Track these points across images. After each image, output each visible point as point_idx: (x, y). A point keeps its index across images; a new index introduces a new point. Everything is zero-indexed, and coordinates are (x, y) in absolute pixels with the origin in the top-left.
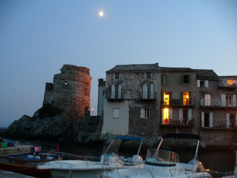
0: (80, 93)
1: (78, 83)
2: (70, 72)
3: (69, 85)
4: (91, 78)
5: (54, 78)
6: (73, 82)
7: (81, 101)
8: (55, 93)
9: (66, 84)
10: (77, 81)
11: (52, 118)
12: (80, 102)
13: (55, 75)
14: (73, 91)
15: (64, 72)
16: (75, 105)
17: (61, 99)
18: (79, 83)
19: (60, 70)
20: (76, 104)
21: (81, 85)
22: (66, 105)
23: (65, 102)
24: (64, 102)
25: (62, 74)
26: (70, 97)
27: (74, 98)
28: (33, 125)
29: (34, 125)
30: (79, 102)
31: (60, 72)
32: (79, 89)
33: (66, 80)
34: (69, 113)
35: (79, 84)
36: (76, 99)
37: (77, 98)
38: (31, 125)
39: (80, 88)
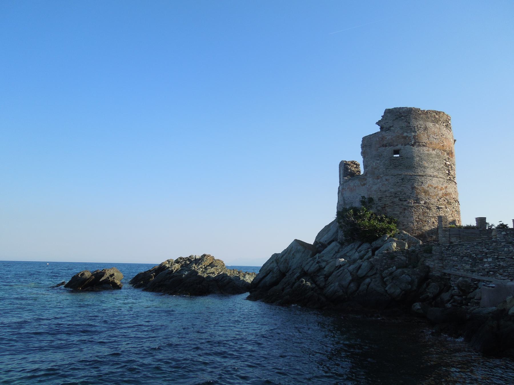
1: (428, 150)
2: (404, 125)
3: (407, 158)
5: (363, 146)
7: (440, 195)
11: (371, 243)
13: (364, 139)
15: (388, 127)
18: (431, 150)
21: (438, 156)
22: (405, 209)
23: (400, 200)
24: (396, 200)
25: (383, 133)
28: (323, 264)
29: (327, 264)
31: (377, 129)
33: (397, 145)
35: (431, 154)
38: (318, 262)
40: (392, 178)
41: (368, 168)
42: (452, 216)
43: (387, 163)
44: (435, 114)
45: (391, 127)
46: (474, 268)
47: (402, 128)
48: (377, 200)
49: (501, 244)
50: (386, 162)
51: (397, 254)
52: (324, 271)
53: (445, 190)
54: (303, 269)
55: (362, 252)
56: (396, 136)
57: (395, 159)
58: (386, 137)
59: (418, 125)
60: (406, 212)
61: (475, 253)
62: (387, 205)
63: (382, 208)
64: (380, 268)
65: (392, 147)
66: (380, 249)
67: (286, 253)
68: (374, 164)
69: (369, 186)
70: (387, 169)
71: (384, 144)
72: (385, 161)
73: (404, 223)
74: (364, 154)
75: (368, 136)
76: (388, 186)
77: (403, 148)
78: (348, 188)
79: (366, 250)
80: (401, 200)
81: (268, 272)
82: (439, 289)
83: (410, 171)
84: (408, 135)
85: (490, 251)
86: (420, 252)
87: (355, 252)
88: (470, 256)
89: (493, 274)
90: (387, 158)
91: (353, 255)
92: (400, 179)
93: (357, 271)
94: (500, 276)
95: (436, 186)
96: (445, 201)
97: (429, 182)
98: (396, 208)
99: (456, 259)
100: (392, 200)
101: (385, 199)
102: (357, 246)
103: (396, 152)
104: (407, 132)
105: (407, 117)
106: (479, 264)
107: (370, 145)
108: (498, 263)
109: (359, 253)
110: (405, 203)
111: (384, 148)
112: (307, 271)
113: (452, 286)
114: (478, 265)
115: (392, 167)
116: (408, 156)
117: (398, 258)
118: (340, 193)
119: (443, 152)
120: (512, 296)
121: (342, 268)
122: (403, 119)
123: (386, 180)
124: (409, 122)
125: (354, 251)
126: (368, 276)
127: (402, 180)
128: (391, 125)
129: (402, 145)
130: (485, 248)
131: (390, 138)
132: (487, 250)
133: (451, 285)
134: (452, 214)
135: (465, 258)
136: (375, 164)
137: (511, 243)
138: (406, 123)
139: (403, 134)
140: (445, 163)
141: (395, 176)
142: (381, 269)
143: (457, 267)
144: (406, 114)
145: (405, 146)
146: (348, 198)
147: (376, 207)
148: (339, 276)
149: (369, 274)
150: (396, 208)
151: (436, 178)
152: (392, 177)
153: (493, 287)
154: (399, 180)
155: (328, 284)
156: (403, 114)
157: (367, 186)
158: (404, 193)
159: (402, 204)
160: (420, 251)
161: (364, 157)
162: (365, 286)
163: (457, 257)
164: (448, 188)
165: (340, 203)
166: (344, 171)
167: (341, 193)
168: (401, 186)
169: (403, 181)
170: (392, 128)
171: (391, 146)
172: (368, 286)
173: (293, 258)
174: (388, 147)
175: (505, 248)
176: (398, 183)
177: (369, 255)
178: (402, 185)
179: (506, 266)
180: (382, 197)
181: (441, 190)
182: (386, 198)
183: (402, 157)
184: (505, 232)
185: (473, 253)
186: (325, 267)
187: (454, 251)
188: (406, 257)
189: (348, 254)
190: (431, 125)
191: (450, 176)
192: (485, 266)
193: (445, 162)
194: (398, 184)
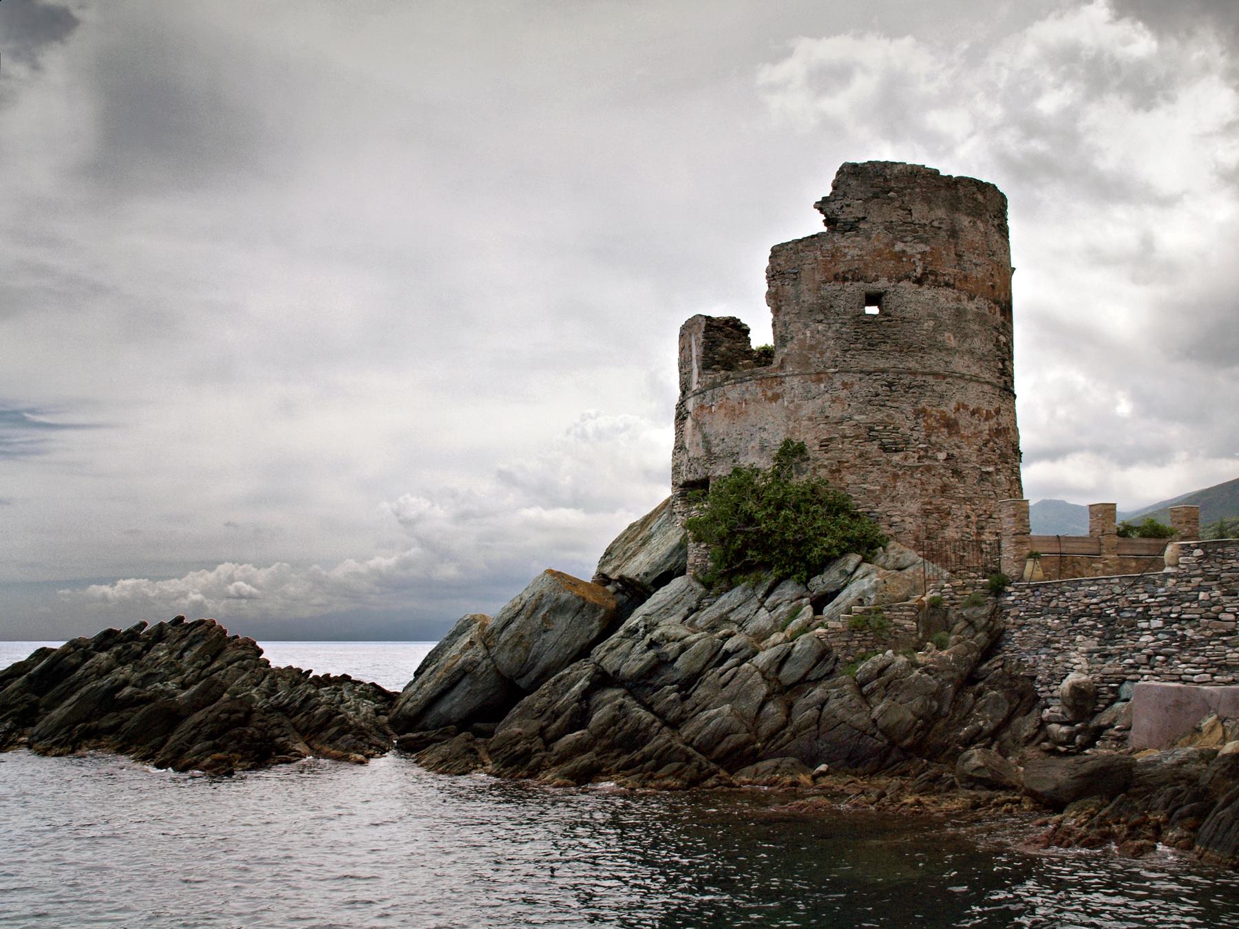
0: (975, 379)
1: (959, 300)
4: (1014, 269)
5: (774, 275)
6: (927, 293)
8: (794, 384)
9: (873, 310)
10: (953, 286)
12: (985, 445)
16: (956, 473)
17: (846, 428)
18: (964, 297)
20: (961, 466)
21: (980, 317)
22: (895, 476)
23: (884, 448)
24: (873, 447)
25: (837, 237)
27: (943, 415)
29: (683, 649)
30: (980, 450)
32: (966, 345)
33: (876, 279)
35: (965, 310)
36: (956, 423)
37: (964, 419)
38: (652, 644)
40: (860, 379)
41: (789, 345)
43: (847, 333)
44: (975, 189)
46: (1109, 647)
48: (817, 448)
49: (1189, 582)
50: (844, 329)
51: (894, 613)
52: (676, 670)
53: (995, 419)
55: (782, 609)
56: (874, 251)
57: (870, 323)
58: (847, 250)
59: (933, 221)
60: (898, 484)
61: (1114, 606)
62: (846, 464)
63: (832, 472)
64: (846, 655)
65: (861, 283)
66: (837, 600)
67: (518, 614)
68: (808, 334)
69: (793, 401)
71: (838, 274)
72: (841, 328)
73: (894, 519)
74: (775, 299)
75: (789, 243)
76: (849, 405)
77: (893, 289)
78: (720, 407)
79: (792, 602)
83: (910, 359)
84: (908, 249)
85: (1159, 599)
86: (953, 605)
87: (759, 608)
88: (1101, 616)
89: (1163, 662)
90: (849, 317)
91: (751, 617)
92: (882, 386)
93: (779, 670)
94: (1184, 666)
96: (994, 451)
98: (871, 472)
99: (1057, 621)
100: (859, 447)
101: (840, 446)
102: (762, 592)
103: (873, 299)
104: (905, 239)
105: (905, 195)
106: (1125, 635)
107: (795, 274)
108: (1179, 633)
109: (770, 611)
110: (896, 458)
113: (1040, 698)
114: (1122, 638)
115: (860, 346)
116: (907, 315)
117: (896, 625)
119: (992, 304)
120: (1215, 716)
121: (730, 662)
123: (845, 385)
124: (910, 210)
125: (754, 605)
126: (809, 681)
127: (888, 389)
128: (861, 216)
129: (890, 280)
130: (1145, 592)
131: (858, 256)
133: (1039, 694)
134: (1009, 490)
135: (1084, 619)
136: (812, 332)
137: (1216, 580)
138: (901, 212)
140: (997, 338)
141: (870, 373)
142: (849, 658)
143: (1057, 645)
144: (902, 186)
145: (899, 282)
146: (722, 437)
147: (814, 469)
148: (725, 685)
149: (813, 676)
150: (871, 472)
151: (975, 385)
152: (860, 375)
154: (879, 387)
155: (693, 709)
156: (893, 184)
157: (786, 403)
158: (894, 428)
159: (889, 462)
160: (953, 602)
161: (776, 310)
163: (1058, 619)
164: (1002, 412)
165: (691, 454)
166: (705, 348)
167: (696, 420)
168: (884, 405)
169: (891, 391)
170: (861, 226)
171: (858, 281)
173: (545, 631)
174: (849, 283)
175: (1199, 591)
177: (805, 618)
178: (889, 404)
179: (1202, 640)
180: (830, 440)
181: (986, 419)
182: (843, 443)
183: (889, 315)
184: (1203, 549)
185: (1109, 606)
186: (675, 659)
187: (1049, 602)
188: (917, 622)
189: (733, 617)
190: (966, 223)
191: (1006, 379)
192: (1141, 640)
193: (996, 334)
194: (877, 398)
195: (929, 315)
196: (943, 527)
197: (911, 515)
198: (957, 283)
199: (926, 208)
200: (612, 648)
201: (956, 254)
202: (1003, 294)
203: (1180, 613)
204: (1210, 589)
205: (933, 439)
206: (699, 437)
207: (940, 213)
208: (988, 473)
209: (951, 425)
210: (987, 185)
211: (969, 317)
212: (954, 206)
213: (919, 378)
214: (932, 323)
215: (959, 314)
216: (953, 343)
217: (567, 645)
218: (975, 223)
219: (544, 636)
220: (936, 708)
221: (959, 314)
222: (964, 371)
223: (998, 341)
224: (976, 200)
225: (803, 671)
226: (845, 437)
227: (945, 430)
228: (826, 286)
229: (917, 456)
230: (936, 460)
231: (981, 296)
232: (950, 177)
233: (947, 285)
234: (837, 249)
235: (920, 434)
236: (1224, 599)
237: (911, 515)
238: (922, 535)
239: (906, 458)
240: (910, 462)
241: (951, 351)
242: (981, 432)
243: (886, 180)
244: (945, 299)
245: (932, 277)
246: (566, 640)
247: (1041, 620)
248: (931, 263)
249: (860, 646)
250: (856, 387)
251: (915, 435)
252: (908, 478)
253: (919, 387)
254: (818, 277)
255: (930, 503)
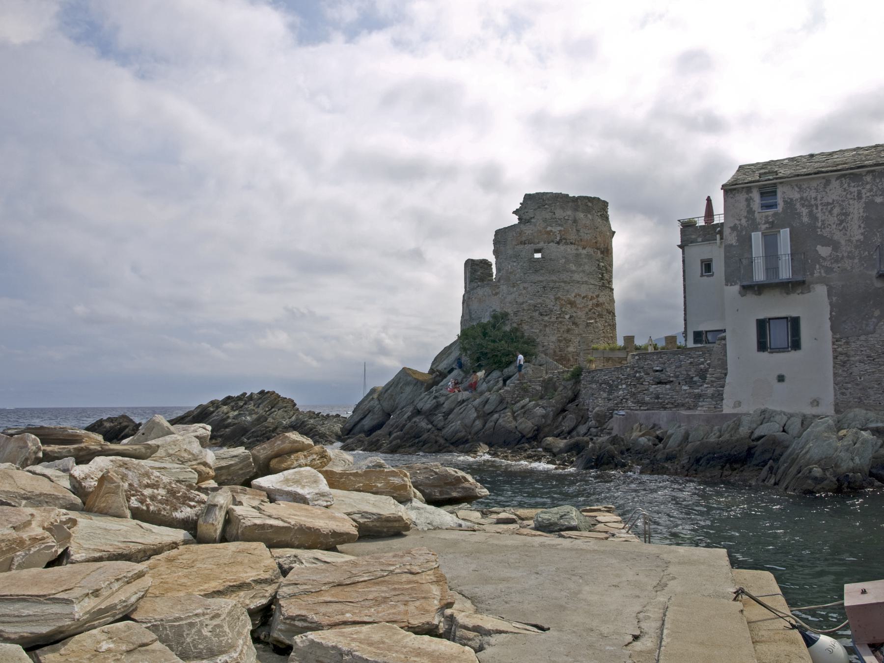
0: (586, 283)
1: (577, 249)
2: (548, 216)
3: (551, 259)
4: (614, 232)
5: (496, 242)
6: (562, 247)
7: (590, 307)
9: (538, 256)
10: (575, 244)
12: (590, 311)
13: (498, 232)
14: (565, 276)
15: (528, 218)
16: (574, 323)
17: (525, 306)
19: (514, 212)
20: (577, 320)
21: (589, 256)
22: (546, 326)
24: (536, 314)
25: (522, 226)
26: (557, 299)
28: (442, 399)
29: (447, 399)
30: (587, 313)
31: (515, 220)
32: (581, 269)
33: (538, 243)
34: (557, 350)
35: (580, 254)
36: (575, 302)
37: (579, 301)
38: (435, 397)
39: (587, 267)
42: (604, 332)
44: (587, 201)
45: (531, 218)
47: (545, 220)
52: (444, 408)
53: (596, 300)
54: (416, 406)
55: (491, 382)
63: (518, 325)
64: (511, 401)
65: (532, 245)
67: (391, 386)
68: (510, 267)
70: (525, 274)
73: (545, 344)
74: (496, 252)
80: (541, 315)
81: (367, 413)
82: (575, 421)
84: (553, 229)
88: (608, 384)
93: (484, 406)
95: (585, 295)
97: (576, 290)
103: (538, 251)
110: (546, 318)
111: (522, 246)
112: (421, 409)
116: (553, 258)
117: (533, 388)
118: (465, 304)
121: (465, 404)
122: (546, 208)
123: (524, 288)
126: (497, 411)
128: (532, 216)
129: (544, 243)
132: (623, 375)
136: (511, 266)
138: (550, 214)
139: (546, 228)
140: (598, 265)
142: (513, 402)
148: (461, 413)
149: (498, 409)
151: (585, 285)
153: (623, 415)
156: (547, 202)
159: (543, 320)
162: (492, 424)
167: (467, 303)
170: (533, 220)
172: (496, 423)
176: (539, 292)
178: (543, 295)
180: (518, 311)
181: (591, 300)
186: (443, 403)
190: (582, 216)
193: (598, 262)
195: (562, 257)
196: (567, 347)
197: (552, 342)
198: (577, 243)
199: (562, 212)
200: (421, 399)
201: (576, 230)
202: (602, 245)
203: (631, 382)
204: (640, 372)
205: (563, 309)
206: (467, 311)
207: (569, 213)
208: (592, 323)
209: (572, 304)
210: (594, 198)
211: (583, 256)
212: (576, 209)
213: (557, 284)
214: (564, 260)
215: (578, 255)
216: (574, 268)
217: (410, 399)
218: (587, 216)
219: (401, 395)
220: (544, 422)
221: (578, 255)
222: (579, 280)
223: (598, 265)
224: (587, 205)
225: (493, 407)
226: (524, 310)
227: (569, 306)
228: (517, 247)
229: (556, 317)
230: (565, 318)
231: (590, 247)
232: (574, 197)
233: (571, 243)
234: (522, 231)
235: (557, 308)
236: (645, 376)
237: (552, 342)
238: (557, 350)
239: (551, 318)
240: (553, 319)
241: (572, 272)
242: (588, 305)
243: (543, 200)
244: (571, 250)
245: (564, 241)
246: (410, 397)
247: (591, 385)
248: (564, 235)
249: (517, 397)
250: (529, 289)
251: (555, 308)
252: (551, 326)
253: (557, 288)
254: (514, 243)
255: (562, 337)
